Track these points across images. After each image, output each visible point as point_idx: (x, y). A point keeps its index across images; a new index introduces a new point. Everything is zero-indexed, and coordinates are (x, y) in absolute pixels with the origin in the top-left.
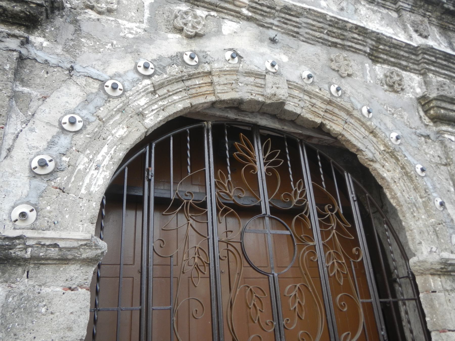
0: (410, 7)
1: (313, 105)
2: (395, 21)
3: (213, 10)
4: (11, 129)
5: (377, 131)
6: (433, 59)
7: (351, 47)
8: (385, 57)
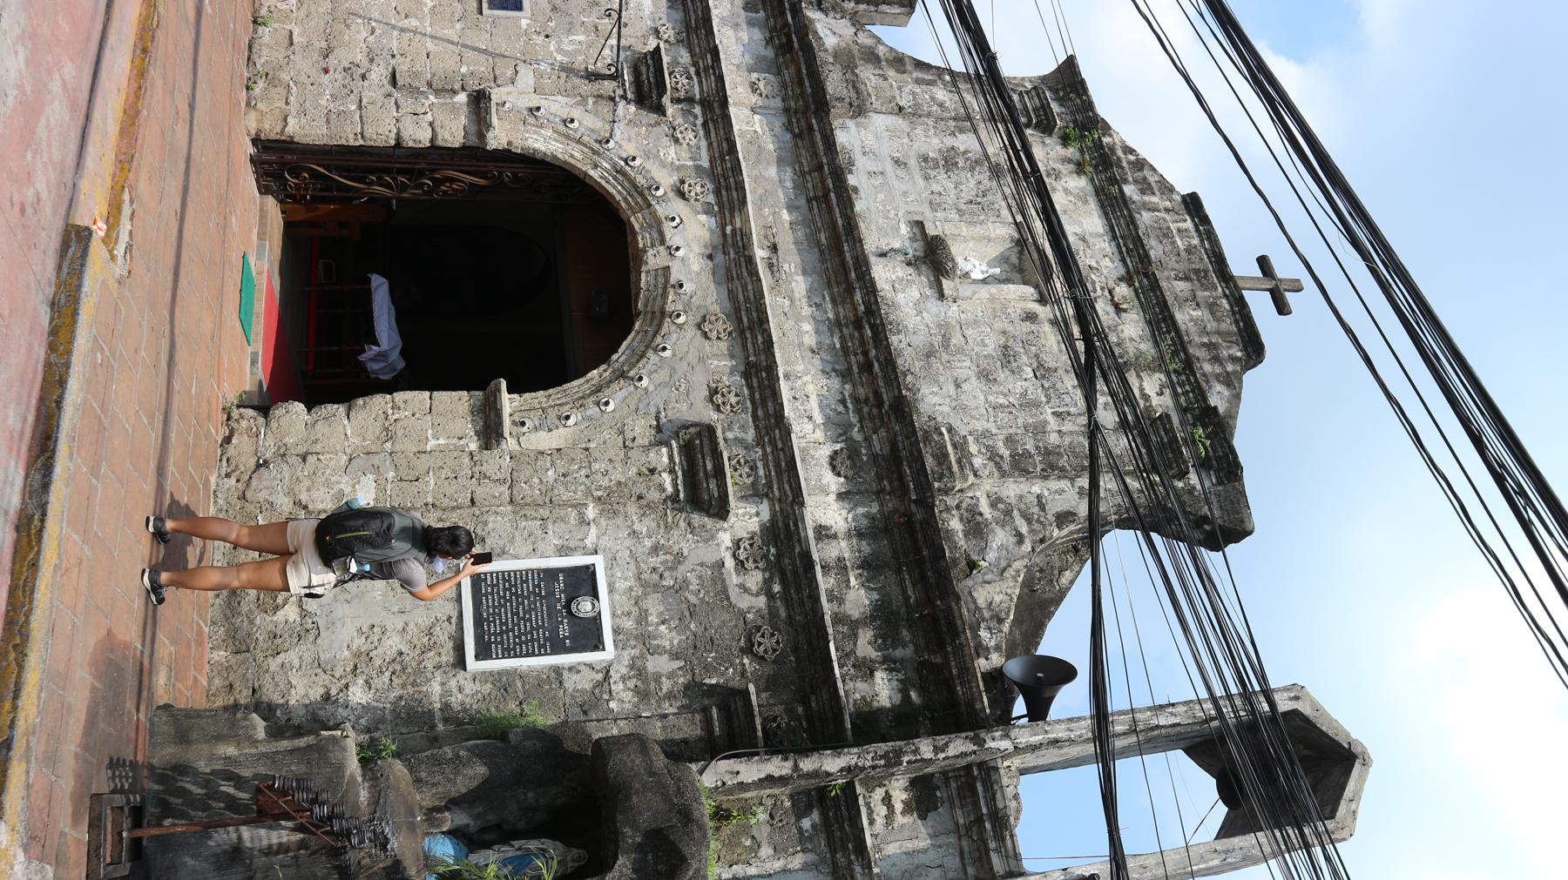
0: (879, 452)
1: (655, 299)
2: (845, 433)
3: (720, 208)
4: (559, 98)
5: (645, 360)
6: (780, 445)
7: (746, 339)
8: (755, 385)
